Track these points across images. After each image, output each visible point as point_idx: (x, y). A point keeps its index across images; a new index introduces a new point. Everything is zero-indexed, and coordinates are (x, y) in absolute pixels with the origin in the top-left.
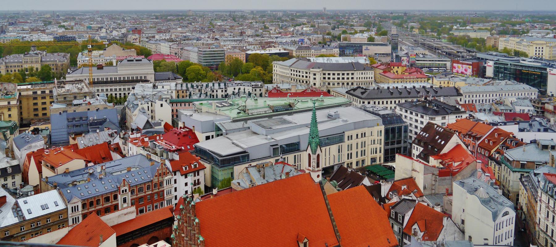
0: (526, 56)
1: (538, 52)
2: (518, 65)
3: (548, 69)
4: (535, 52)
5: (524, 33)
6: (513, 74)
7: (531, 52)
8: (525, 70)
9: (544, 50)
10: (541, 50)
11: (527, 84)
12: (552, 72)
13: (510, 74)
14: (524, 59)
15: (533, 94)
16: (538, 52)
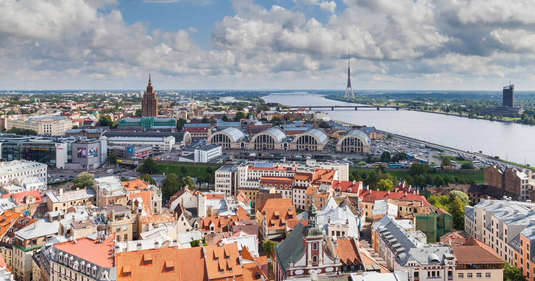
0: (35, 134)
1: (46, 130)
2: (28, 144)
3: (56, 144)
4: (44, 130)
5: (32, 112)
6: (23, 153)
7: (41, 130)
8: (34, 148)
9: (52, 127)
10: (49, 127)
11: (37, 161)
12: (60, 147)
13: (19, 153)
14: (33, 137)
15: (43, 170)
16: (46, 130)
